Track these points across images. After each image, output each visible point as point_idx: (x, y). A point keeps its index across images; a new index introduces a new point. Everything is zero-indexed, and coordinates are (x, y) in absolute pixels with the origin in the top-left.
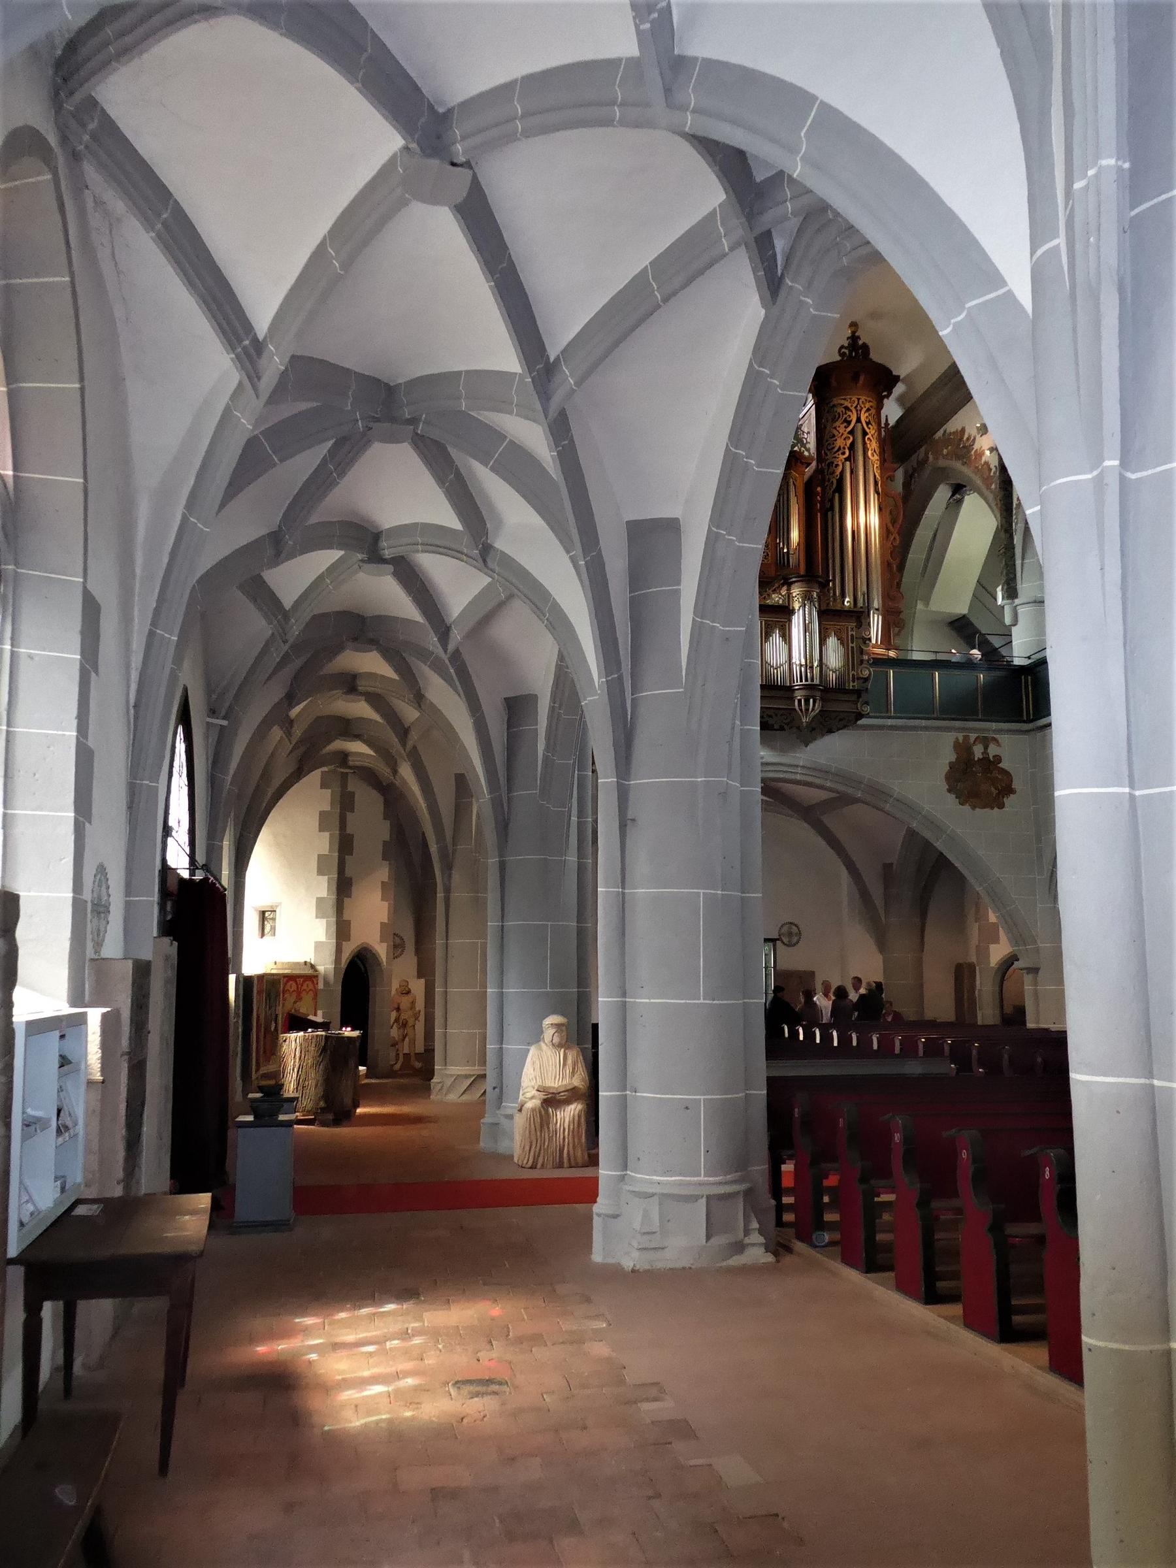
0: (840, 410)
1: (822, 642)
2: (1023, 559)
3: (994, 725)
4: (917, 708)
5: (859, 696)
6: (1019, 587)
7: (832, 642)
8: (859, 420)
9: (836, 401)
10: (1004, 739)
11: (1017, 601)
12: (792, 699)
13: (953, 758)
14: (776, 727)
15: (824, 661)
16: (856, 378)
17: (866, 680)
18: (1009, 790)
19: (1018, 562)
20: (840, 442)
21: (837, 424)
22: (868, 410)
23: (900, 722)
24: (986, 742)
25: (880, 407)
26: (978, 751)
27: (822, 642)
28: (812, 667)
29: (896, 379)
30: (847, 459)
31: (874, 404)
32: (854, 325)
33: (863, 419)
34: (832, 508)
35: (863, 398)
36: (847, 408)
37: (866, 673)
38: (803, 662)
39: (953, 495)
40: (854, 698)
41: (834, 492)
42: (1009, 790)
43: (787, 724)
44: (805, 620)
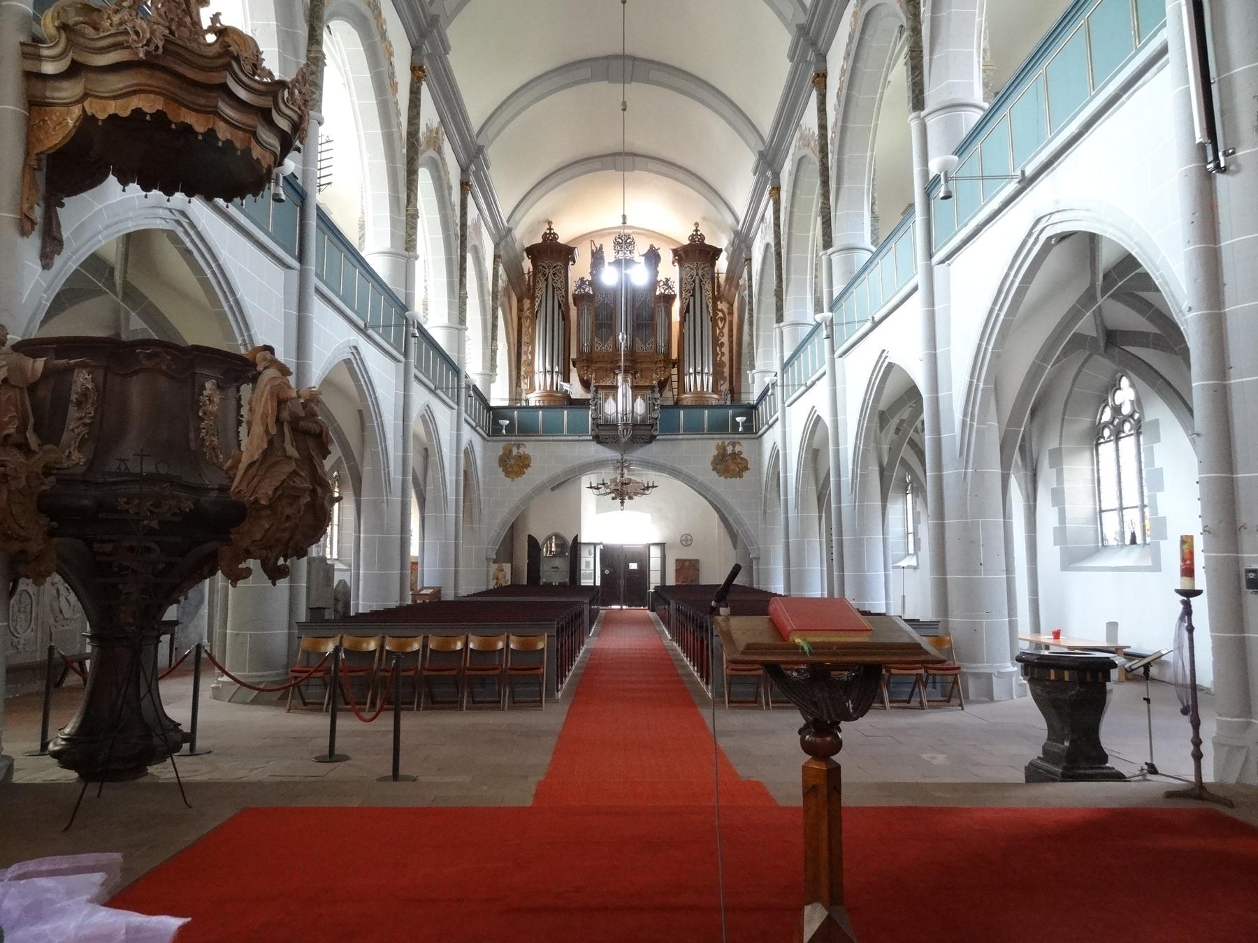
1: (634, 401)
4: (695, 429)
7: (639, 401)
10: (744, 442)
13: (715, 453)
18: (746, 468)
24: (734, 445)
25: (713, 265)
26: (729, 450)
27: (634, 401)
29: (721, 250)
42: (746, 468)
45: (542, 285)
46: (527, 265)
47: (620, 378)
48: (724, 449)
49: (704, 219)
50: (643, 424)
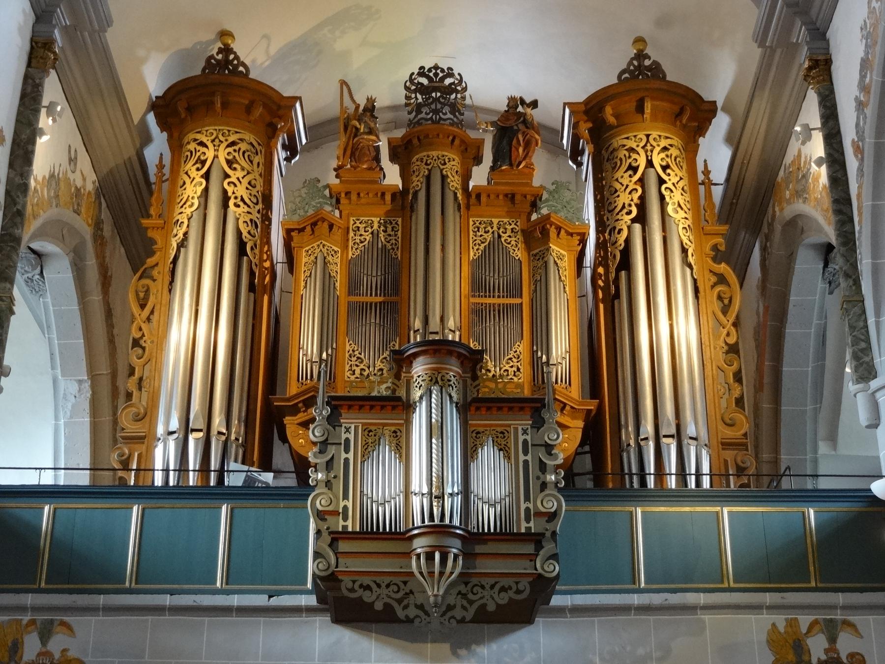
0: (623, 153)
1: (469, 455)
2: (878, 314)
3: (840, 598)
5: (539, 546)
6: (877, 361)
7: (488, 455)
8: (650, 164)
9: (618, 141)
10: (867, 622)
11: (874, 384)
12: (407, 555)
14: (379, 606)
15: (474, 486)
16: (640, 109)
17: (552, 516)
19: (871, 321)
20: (623, 198)
21: (619, 174)
22: (665, 149)
23: (657, 599)
24: (831, 630)
25: (690, 149)
26: (817, 646)
27: (469, 455)
28: (441, 497)
30: (634, 221)
31: (676, 141)
32: (639, 40)
33: (657, 161)
34: (617, 295)
35: (654, 134)
36: (631, 150)
37: (551, 505)
38: (425, 490)
39: (826, 265)
40: (529, 549)
41: (618, 271)
43: (399, 601)
44: (430, 417)
45: (193, 190)
46: (157, 148)
47: (420, 369)
48: (799, 647)
49: (663, 22)
50: (504, 534)
